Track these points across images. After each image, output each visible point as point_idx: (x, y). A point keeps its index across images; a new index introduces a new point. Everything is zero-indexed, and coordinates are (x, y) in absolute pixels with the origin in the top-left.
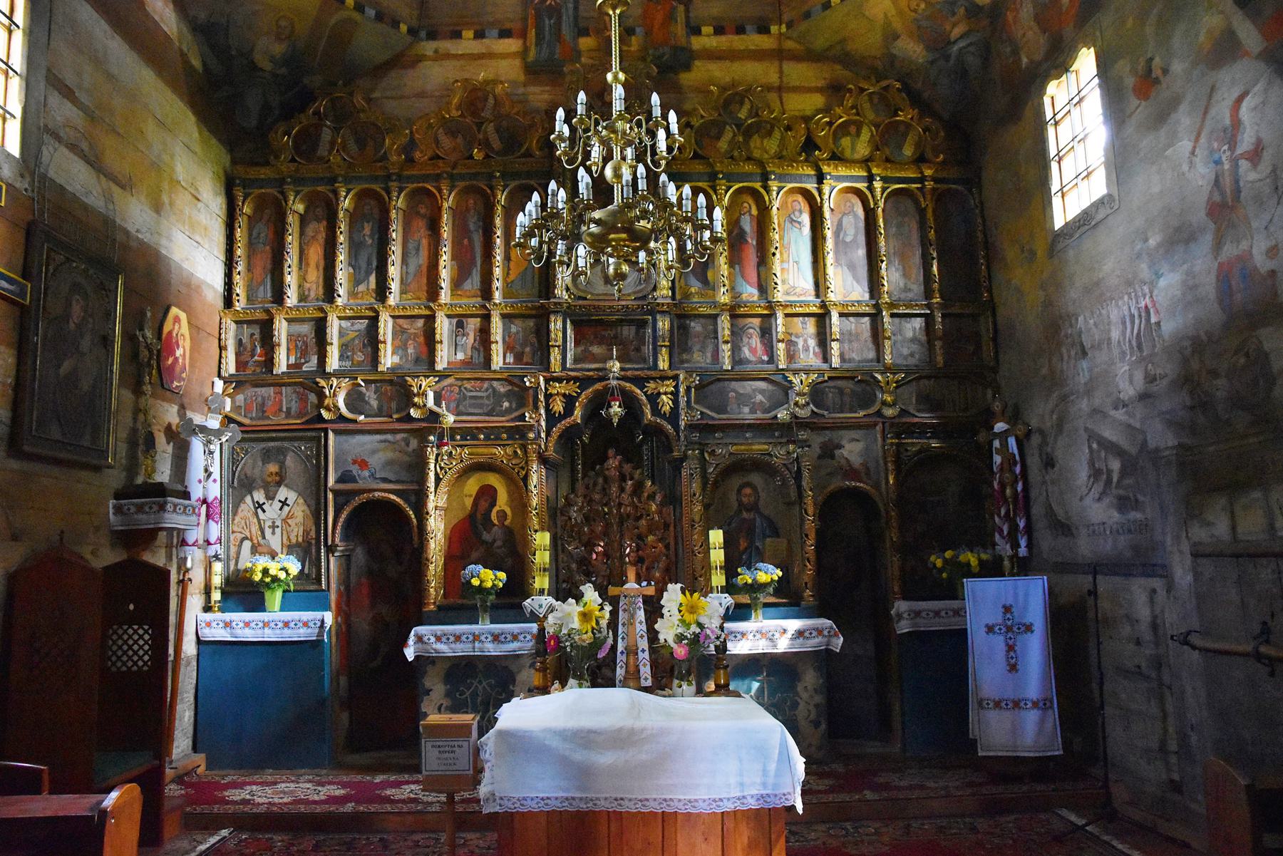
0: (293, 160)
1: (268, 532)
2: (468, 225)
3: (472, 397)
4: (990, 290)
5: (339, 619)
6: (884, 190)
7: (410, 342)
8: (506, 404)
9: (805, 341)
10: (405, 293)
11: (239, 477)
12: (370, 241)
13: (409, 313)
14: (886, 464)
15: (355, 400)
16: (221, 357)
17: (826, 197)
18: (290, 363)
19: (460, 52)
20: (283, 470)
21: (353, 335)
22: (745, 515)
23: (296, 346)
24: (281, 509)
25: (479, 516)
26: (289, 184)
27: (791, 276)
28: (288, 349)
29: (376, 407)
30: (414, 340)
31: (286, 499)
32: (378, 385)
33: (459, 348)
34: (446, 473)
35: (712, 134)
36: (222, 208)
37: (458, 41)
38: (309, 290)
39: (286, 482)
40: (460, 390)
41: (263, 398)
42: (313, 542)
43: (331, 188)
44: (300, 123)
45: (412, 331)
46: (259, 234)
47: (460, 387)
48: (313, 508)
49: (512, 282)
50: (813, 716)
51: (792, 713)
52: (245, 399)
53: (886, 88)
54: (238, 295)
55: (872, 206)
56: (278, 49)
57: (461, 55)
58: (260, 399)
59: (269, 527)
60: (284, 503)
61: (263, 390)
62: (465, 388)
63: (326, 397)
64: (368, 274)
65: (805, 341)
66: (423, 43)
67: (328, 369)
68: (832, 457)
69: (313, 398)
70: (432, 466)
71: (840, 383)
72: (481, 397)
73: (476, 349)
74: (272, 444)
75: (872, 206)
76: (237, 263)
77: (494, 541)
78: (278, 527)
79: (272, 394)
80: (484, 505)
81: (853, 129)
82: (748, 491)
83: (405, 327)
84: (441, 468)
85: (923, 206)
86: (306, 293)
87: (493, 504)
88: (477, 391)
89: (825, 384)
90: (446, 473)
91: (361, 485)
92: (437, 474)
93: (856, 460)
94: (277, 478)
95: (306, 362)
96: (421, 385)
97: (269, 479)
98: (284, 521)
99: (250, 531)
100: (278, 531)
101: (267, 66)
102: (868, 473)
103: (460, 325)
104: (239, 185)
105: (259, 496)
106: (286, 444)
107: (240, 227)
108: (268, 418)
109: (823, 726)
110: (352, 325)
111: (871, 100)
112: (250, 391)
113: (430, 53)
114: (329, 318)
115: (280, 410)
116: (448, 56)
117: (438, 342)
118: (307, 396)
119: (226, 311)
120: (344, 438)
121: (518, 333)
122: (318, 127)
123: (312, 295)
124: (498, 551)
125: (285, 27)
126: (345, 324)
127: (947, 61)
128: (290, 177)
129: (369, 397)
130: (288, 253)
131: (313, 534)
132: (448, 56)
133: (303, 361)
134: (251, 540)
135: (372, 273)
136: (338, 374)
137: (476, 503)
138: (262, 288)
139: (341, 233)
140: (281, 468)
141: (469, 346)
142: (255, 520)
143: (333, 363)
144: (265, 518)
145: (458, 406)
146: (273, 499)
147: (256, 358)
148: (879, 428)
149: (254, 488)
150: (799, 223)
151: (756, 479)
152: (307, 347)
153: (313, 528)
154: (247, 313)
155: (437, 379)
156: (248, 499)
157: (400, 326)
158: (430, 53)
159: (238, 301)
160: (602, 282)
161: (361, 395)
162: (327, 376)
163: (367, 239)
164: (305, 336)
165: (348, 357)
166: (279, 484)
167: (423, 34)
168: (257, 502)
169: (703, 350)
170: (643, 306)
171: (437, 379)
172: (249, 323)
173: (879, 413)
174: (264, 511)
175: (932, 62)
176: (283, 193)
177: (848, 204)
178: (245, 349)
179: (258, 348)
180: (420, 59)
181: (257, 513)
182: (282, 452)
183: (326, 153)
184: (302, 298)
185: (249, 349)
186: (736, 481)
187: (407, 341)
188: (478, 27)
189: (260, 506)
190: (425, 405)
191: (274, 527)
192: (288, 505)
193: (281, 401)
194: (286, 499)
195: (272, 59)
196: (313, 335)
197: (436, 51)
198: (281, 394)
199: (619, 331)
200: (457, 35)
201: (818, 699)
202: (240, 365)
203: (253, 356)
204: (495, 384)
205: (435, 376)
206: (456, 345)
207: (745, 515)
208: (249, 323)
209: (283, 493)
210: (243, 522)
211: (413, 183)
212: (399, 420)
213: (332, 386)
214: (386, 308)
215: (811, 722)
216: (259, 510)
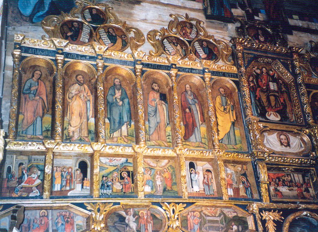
2: (188, 101)
7: (157, 176)
10: (149, 141)
21: (112, 169)
23: (62, 175)
29: (135, 228)
30: (160, 174)
32: (136, 209)
33: (194, 182)
38: (73, 132)
40: (201, 214)
45: (158, 168)
47: (200, 212)
49: (222, 139)
57: (167, 4)
62: (205, 215)
64: (121, 124)
73: (206, 184)
79: (38, 217)
86: (71, 134)
88: (213, 216)
95: (71, 190)
110: (111, 161)
129: (129, 220)
133: (68, 188)
135: (123, 124)
138: (31, 128)
147: (23, 184)
152: (71, 177)
157: (149, 165)
160: (279, 143)
163: (118, 100)
164: (70, 168)
165: (108, 186)
171: (185, 205)
178: (13, 176)
179: (26, 175)
185: (17, 176)
187: (155, 176)
193: (47, 224)
196: (77, 167)
198: (47, 216)
205: (183, 203)
206: (191, 180)
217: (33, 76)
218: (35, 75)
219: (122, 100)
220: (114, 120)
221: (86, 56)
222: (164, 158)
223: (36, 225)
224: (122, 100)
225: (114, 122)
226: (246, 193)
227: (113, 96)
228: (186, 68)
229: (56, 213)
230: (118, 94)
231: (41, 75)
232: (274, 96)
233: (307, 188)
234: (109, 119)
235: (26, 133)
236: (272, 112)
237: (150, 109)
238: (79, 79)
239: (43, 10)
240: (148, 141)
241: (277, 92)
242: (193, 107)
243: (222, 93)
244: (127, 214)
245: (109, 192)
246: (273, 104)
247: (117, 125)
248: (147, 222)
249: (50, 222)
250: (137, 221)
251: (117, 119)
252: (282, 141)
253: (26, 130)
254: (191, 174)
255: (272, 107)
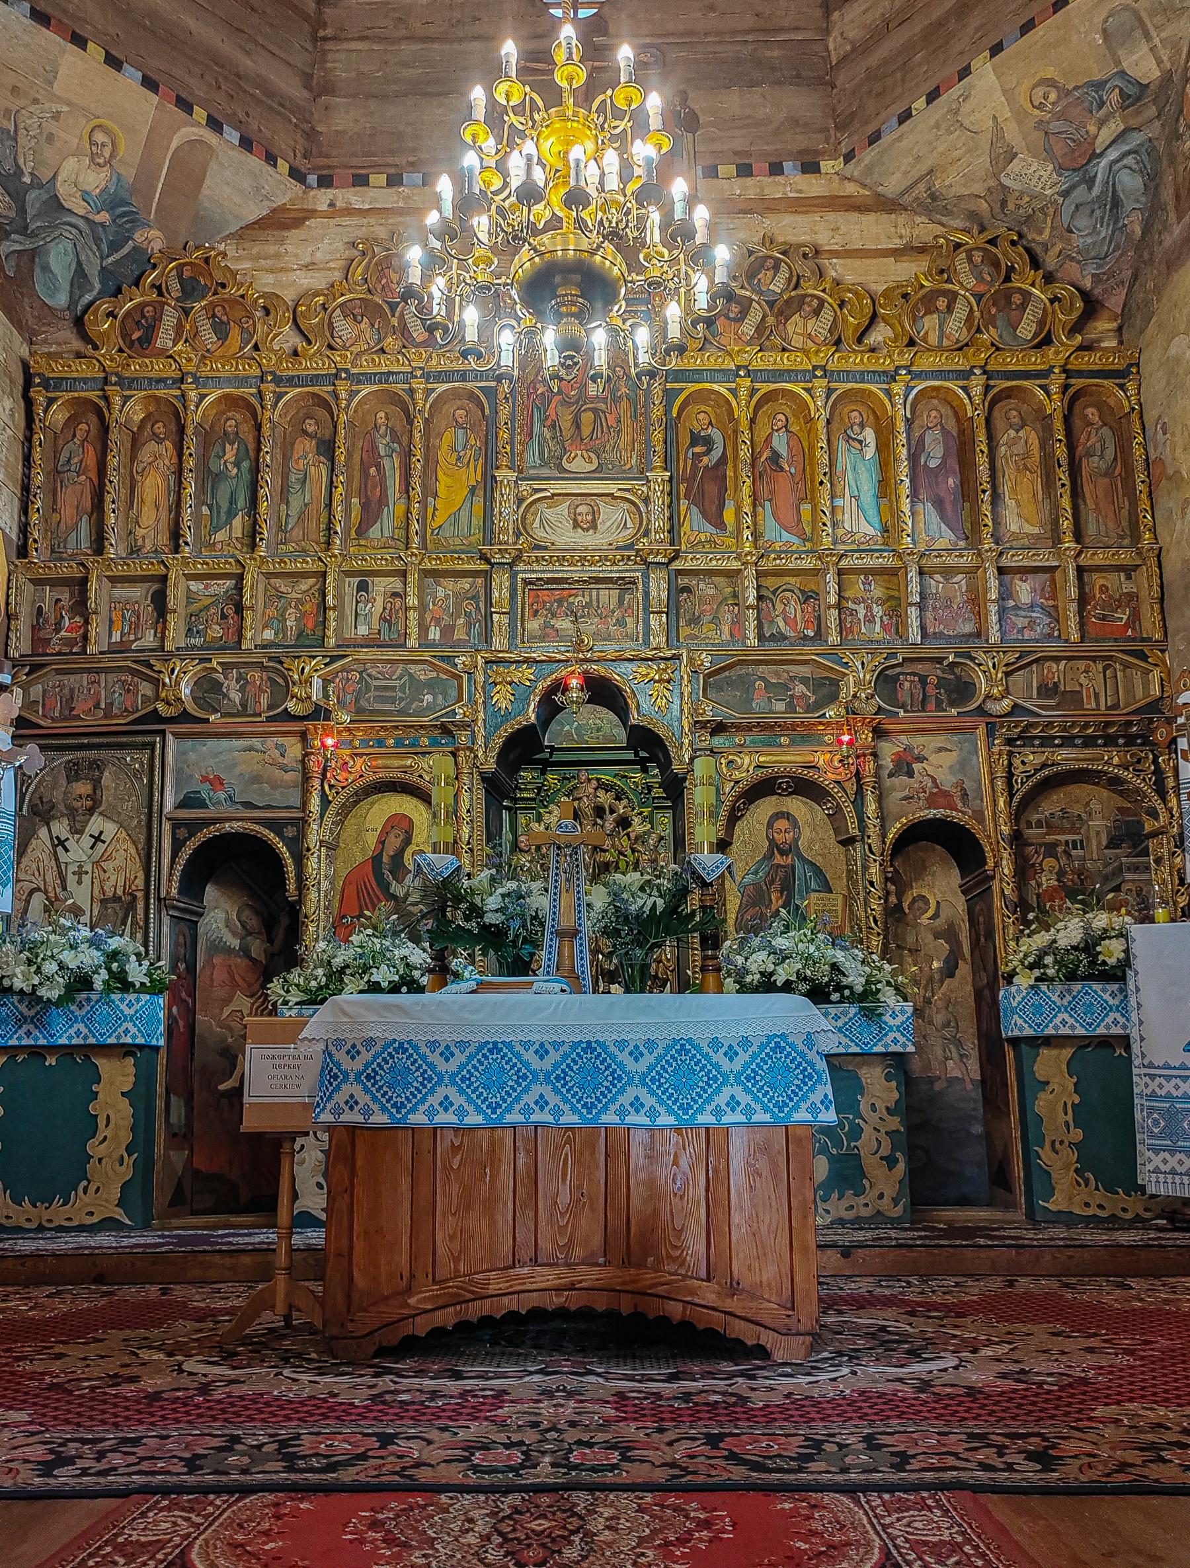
0: (121, 350)
1: (71, 879)
2: (377, 448)
3: (377, 688)
4: (1153, 530)
5: (175, 1009)
6: (987, 388)
8: (428, 698)
9: (869, 608)
11: (30, 800)
12: (235, 470)
13: (290, 567)
14: (992, 781)
15: (208, 688)
16: (9, 629)
17: (899, 400)
18: (113, 640)
19: (367, 207)
20: (98, 792)
22: (778, 859)
23: (123, 616)
24: (92, 848)
25: (385, 859)
26: (115, 384)
27: (847, 516)
28: (111, 621)
30: (296, 607)
31: (101, 832)
34: (337, 793)
35: (732, 315)
36: (12, 416)
37: (365, 189)
39: (101, 809)
41: (72, 690)
42: (140, 895)
43: (178, 393)
44: (131, 300)
45: (294, 595)
46: (70, 459)
47: (361, 673)
48: (140, 847)
49: (440, 527)
50: (885, 1151)
51: (852, 1144)
52: (45, 691)
53: (992, 242)
54: (35, 541)
55: (970, 414)
56: (95, 180)
58: (66, 691)
59: (74, 873)
60: (97, 839)
61: (72, 677)
62: (369, 675)
63: (164, 684)
64: (231, 515)
65: (869, 608)
66: (312, 193)
67: (169, 646)
68: (910, 774)
69: (146, 689)
70: (316, 783)
71: (919, 668)
72: (393, 688)
73: (385, 620)
74: (80, 754)
75: (970, 414)
76: (35, 496)
77: (407, 895)
78: (87, 873)
79: (85, 683)
80: (394, 843)
81: (942, 303)
82: (782, 824)
83: (283, 589)
84: (331, 787)
85: (1049, 412)
87: (408, 841)
89: (898, 670)
90: (337, 793)
91: (211, 812)
92: (323, 795)
93: (947, 780)
94: (89, 803)
96: (303, 669)
97: (77, 804)
98: (96, 863)
99: (44, 880)
100: (86, 879)
101: (80, 207)
102: (964, 795)
103: (363, 587)
104: (39, 385)
105: (60, 828)
106: (103, 754)
107: (40, 445)
108: (78, 718)
109: (901, 1166)
111: (970, 259)
112: (53, 680)
113: (323, 207)
114: (172, 575)
115: (97, 706)
116: (349, 211)
117: (330, 609)
118: (136, 685)
119: (17, 562)
120: (189, 743)
121: (447, 597)
122: (159, 307)
123: (148, 546)
124: (410, 908)
125: (103, 145)
126: (195, 586)
127: (1090, 189)
128: (117, 374)
130: (111, 482)
131: (140, 883)
132: (349, 211)
133: (132, 637)
134: (46, 893)
135: (236, 514)
136: (181, 653)
137: (381, 842)
139: (191, 455)
140: (94, 790)
141: (376, 616)
142: (53, 862)
143: (176, 636)
144: (69, 860)
145: (357, 700)
146: (81, 832)
147: (63, 633)
148: (981, 731)
149: (54, 818)
150: (860, 442)
151: (797, 806)
152: (138, 619)
153: (141, 875)
154: (49, 568)
155: (328, 660)
156: (43, 832)
158: (323, 207)
159: (36, 550)
161: (216, 687)
162: (167, 658)
163: (230, 467)
166: (91, 811)
167: (312, 179)
168: (57, 838)
169: (716, 620)
170: (629, 557)
172: (55, 583)
173: (981, 711)
174: (67, 850)
175: (1065, 194)
176: (106, 398)
177: (934, 413)
178: (46, 620)
179: (67, 619)
180: (312, 213)
181: (55, 852)
182: (97, 766)
183: (170, 344)
184: (134, 551)
185: (52, 620)
186: (765, 807)
187: (285, 610)
188: (392, 171)
189: (62, 843)
190: (309, 698)
191: (80, 873)
192: (104, 842)
194: (101, 832)
195: (85, 196)
197: (332, 205)
198: (99, 681)
199: (594, 597)
200: (361, 181)
201: (895, 1123)
202: (39, 642)
203: (57, 631)
204: (412, 668)
207: (778, 859)
208: (55, 583)
209: (96, 824)
210: (34, 866)
211: (296, 386)
212: (270, 719)
213: (173, 670)
214: (255, 559)
215: (881, 1158)
216: (60, 849)
217: (74, 436)
218: (78, 433)
219: (237, 464)
220: (219, 507)
221: (167, 379)
222: (305, 575)
223: (82, 697)
224: (237, 464)
225: (219, 512)
226: (468, 634)
227: (220, 458)
228: (375, 374)
229: (112, 677)
230: (230, 453)
231: (88, 432)
232: (595, 411)
233: (623, 618)
234: (210, 508)
235: (65, 547)
236: (579, 453)
237: (293, 478)
238: (157, 431)
239: (91, 291)
240: (282, 543)
241: (604, 400)
242: (386, 463)
243: (460, 420)
244: (226, 678)
245: (199, 641)
246: (586, 432)
247: (223, 517)
248: (261, 690)
249: (103, 692)
250: (242, 690)
251: (225, 506)
252: (579, 518)
253: (65, 540)
254: (357, 602)
255: (582, 439)
